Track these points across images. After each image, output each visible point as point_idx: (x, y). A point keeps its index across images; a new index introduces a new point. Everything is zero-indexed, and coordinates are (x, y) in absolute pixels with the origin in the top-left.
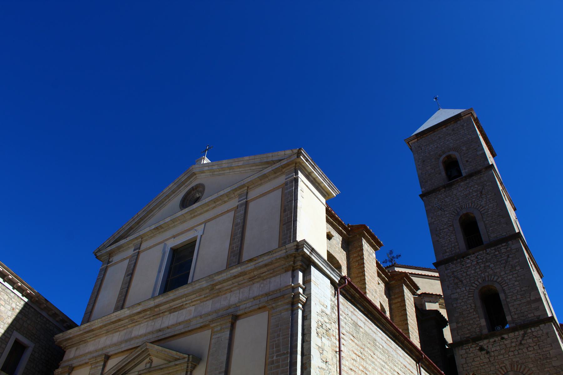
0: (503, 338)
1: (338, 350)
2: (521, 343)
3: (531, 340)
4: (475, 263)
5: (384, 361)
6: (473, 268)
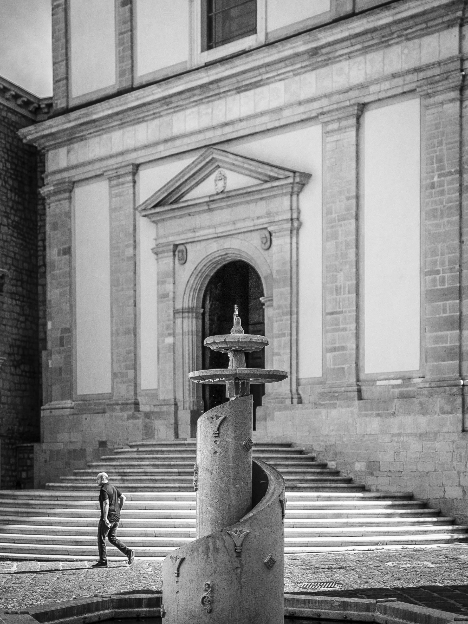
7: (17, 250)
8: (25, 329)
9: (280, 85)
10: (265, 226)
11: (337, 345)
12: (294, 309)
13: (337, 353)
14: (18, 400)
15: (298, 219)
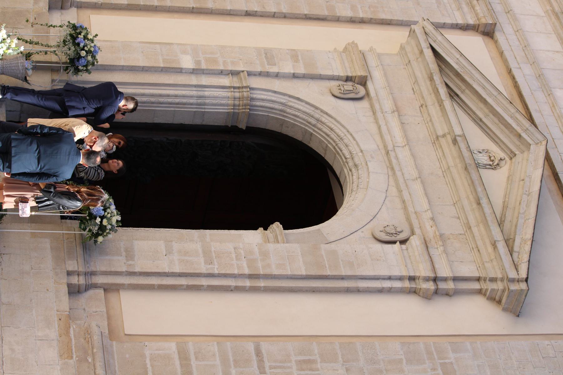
10: (417, 231)
11: (194, 363)
12: (262, 283)
13: (177, 363)
15: (437, 292)
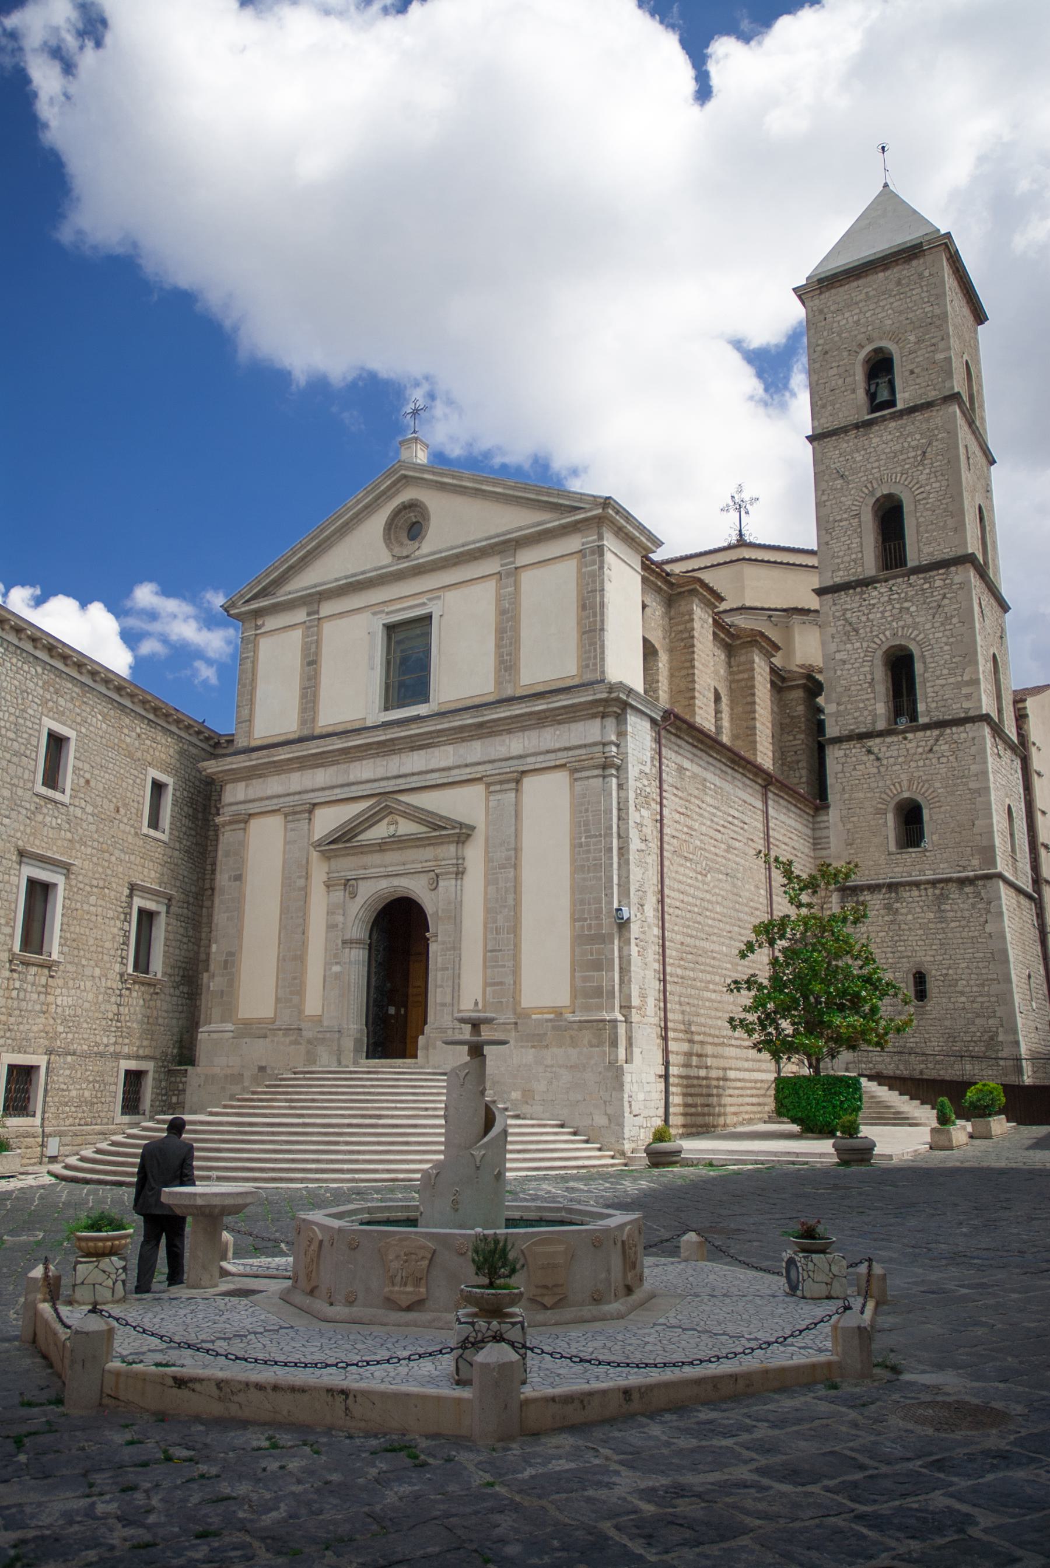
0: (905, 738)
1: (658, 817)
2: (931, 750)
3: (946, 747)
4: (886, 598)
5: (715, 808)
6: (881, 609)
7: (186, 873)
8: (188, 950)
9: (450, 749)
14: (174, 1021)
